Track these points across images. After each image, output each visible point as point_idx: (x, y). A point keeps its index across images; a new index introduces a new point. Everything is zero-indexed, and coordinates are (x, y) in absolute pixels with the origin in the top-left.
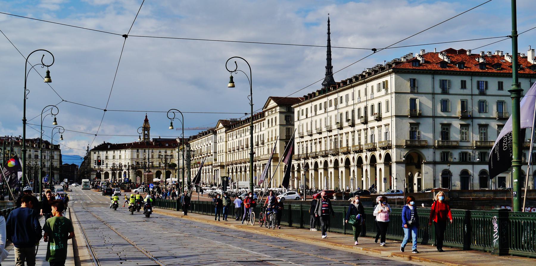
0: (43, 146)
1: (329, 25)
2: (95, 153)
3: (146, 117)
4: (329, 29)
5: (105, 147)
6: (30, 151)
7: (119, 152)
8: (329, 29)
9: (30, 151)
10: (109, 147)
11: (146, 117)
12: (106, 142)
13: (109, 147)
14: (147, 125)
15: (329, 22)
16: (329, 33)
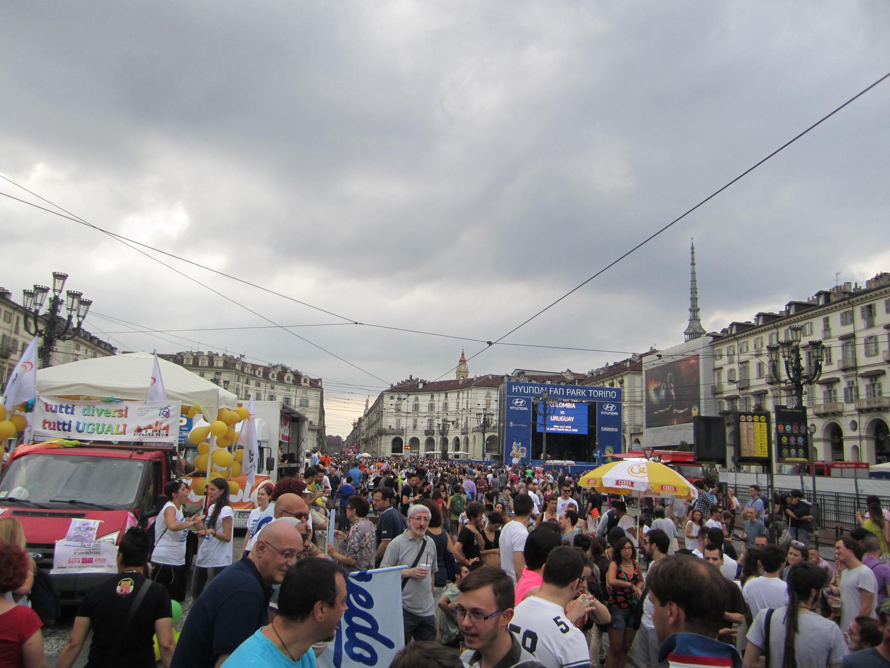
0: (288, 379)
1: (693, 253)
2: (392, 398)
3: (463, 355)
4: (693, 259)
5: (409, 387)
6: (258, 385)
7: (443, 395)
8: (693, 259)
9: (258, 385)
10: (421, 386)
11: (463, 355)
12: (414, 378)
13: (421, 386)
14: (463, 367)
15: (693, 248)
16: (693, 264)
